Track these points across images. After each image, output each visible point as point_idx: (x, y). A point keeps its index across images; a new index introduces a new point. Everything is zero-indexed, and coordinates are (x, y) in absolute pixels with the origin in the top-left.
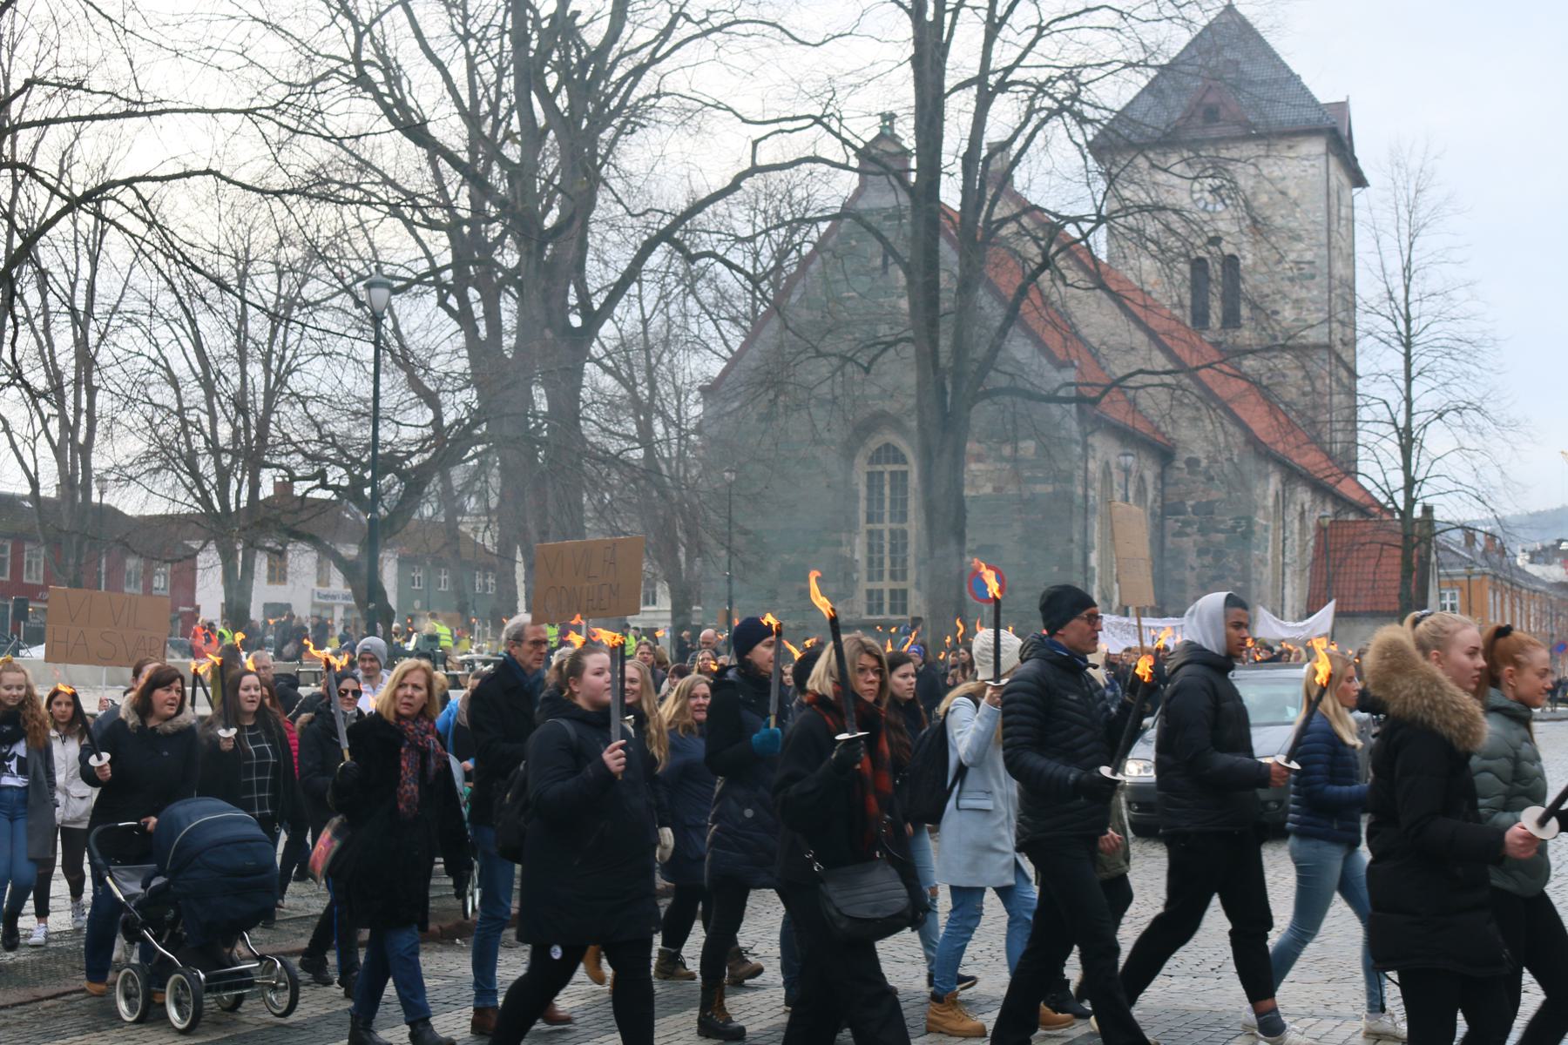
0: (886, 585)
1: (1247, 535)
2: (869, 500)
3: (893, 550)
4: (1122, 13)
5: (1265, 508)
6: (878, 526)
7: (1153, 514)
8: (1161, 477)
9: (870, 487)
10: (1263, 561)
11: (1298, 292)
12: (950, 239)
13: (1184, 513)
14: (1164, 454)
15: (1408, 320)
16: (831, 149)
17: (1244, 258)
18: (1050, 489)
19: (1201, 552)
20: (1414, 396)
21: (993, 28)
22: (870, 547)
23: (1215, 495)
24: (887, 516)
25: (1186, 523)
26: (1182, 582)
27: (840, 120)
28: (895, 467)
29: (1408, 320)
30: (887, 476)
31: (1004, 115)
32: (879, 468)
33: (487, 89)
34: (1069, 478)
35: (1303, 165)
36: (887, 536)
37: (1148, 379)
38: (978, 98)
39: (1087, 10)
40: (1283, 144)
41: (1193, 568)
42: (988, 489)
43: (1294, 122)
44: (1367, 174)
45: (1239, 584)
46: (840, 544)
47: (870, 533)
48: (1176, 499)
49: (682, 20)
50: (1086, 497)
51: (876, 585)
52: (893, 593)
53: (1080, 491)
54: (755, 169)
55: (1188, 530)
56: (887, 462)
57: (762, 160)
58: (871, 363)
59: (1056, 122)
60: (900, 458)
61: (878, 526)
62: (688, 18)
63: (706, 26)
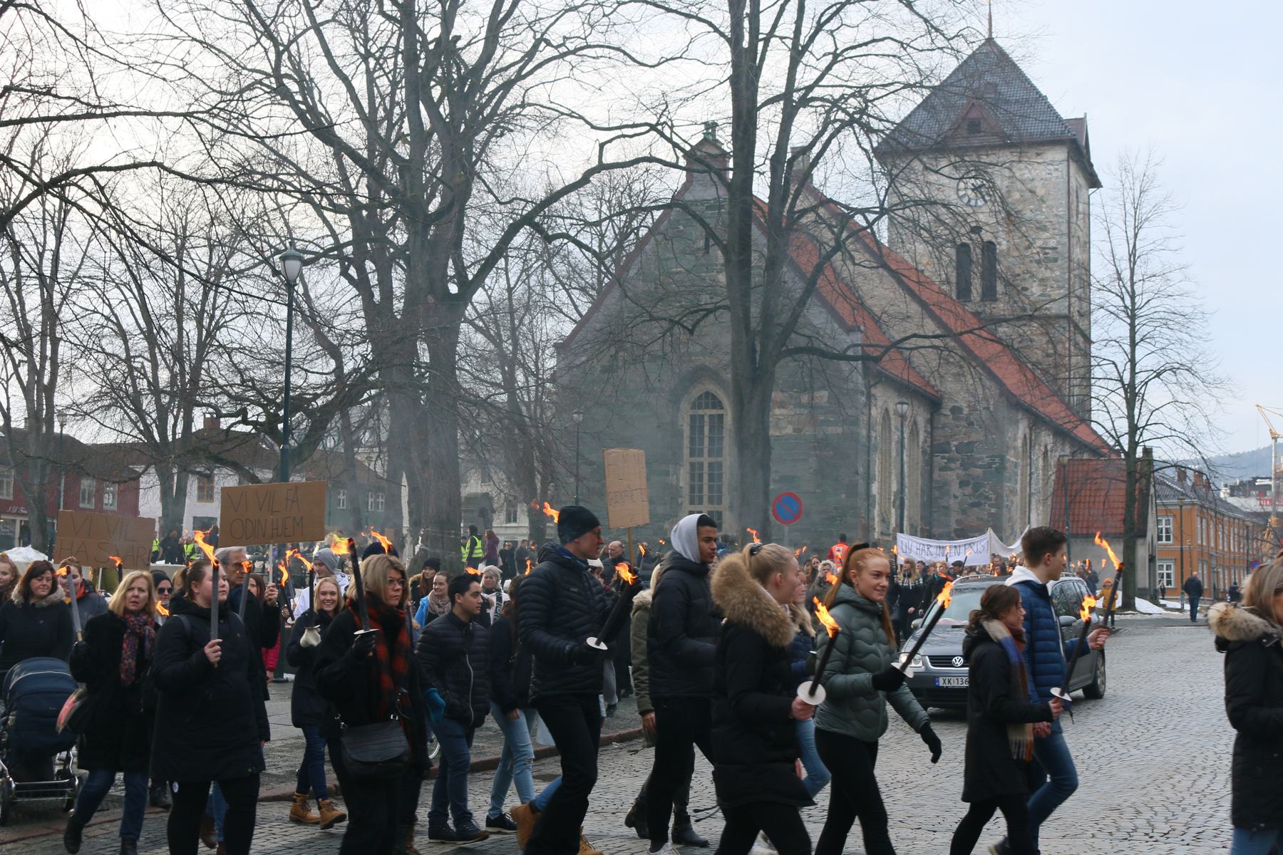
1: (1001, 469)
2: (692, 440)
3: (711, 478)
4: (902, 43)
5: (1015, 448)
6: (700, 459)
7: (924, 452)
8: (931, 421)
9: (692, 428)
10: (1013, 492)
12: (760, 225)
14: (934, 403)
15: (1133, 297)
16: (664, 151)
17: (1000, 244)
18: (840, 430)
19: (963, 484)
20: (1137, 359)
21: (797, 54)
22: (692, 477)
23: (974, 437)
24: (706, 451)
25: (951, 460)
26: (947, 508)
27: (671, 127)
28: (714, 412)
29: (1133, 297)
30: (706, 419)
31: (805, 125)
32: (701, 412)
33: (383, 99)
34: (855, 422)
35: (1048, 169)
37: (921, 342)
38: (784, 110)
39: (874, 41)
40: (1032, 152)
41: (956, 497)
42: (789, 430)
43: (1042, 134)
44: (1101, 177)
45: (993, 510)
47: (692, 465)
48: (943, 440)
49: (543, 44)
50: (869, 437)
53: (864, 432)
54: (601, 167)
55: (953, 465)
56: (707, 407)
57: (609, 158)
58: (694, 326)
59: (847, 132)
60: (717, 404)
62: (548, 43)
63: (563, 50)
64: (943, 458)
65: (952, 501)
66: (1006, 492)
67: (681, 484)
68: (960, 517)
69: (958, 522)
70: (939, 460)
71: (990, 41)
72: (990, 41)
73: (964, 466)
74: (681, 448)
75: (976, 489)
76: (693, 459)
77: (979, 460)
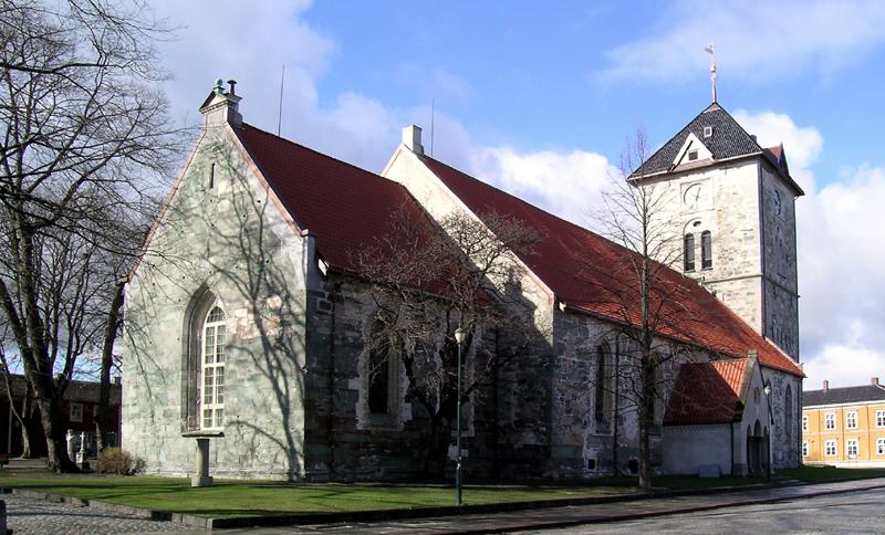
11: (744, 247)
19: (521, 382)
26: (509, 403)
41: (515, 393)
48: (505, 346)
69: (517, 414)
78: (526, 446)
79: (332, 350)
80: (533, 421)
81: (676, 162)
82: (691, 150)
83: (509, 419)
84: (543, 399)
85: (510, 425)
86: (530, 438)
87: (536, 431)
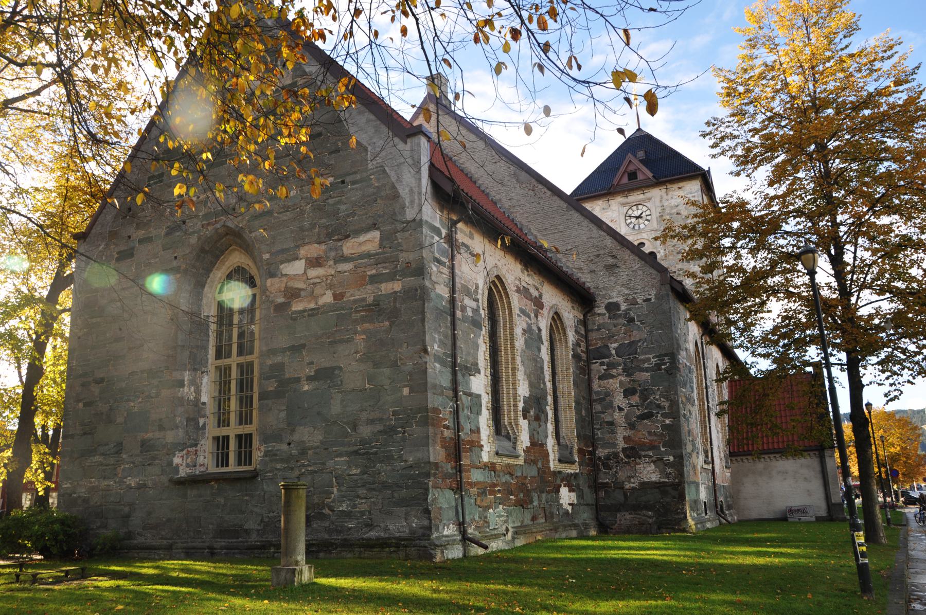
0: (233, 430)
5: (687, 350)
7: (576, 356)
8: (584, 323)
10: (689, 400)
13: (609, 356)
14: (583, 298)
18: (397, 286)
19: (628, 393)
23: (636, 335)
25: (611, 366)
26: (611, 423)
36: (234, 373)
41: (621, 409)
42: (327, 298)
45: (667, 422)
46: (181, 384)
51: (224, 431)
52: (239, 437)
55: (614, 372)
61: (227, 361)
64: (602, 364)
65: (617, 415)
66: (682, 399)
67: (204, 398)
68: (628, 433)
70: (597, 368)
71: (639, 129)
72: (639, 129)
73: (628, 371)
74: (205, 348)
75: (644, 396)
76: (220, 362)
77: (644, 361)
78: (645, 486)
79: (453, 324)
80: (653, 447)
81: (615, 182)
82: (631, 168)
83: (614, 445)
84: (665, 416)
85: (616, 455)
86: (649, 473)
87: (658, 462)
